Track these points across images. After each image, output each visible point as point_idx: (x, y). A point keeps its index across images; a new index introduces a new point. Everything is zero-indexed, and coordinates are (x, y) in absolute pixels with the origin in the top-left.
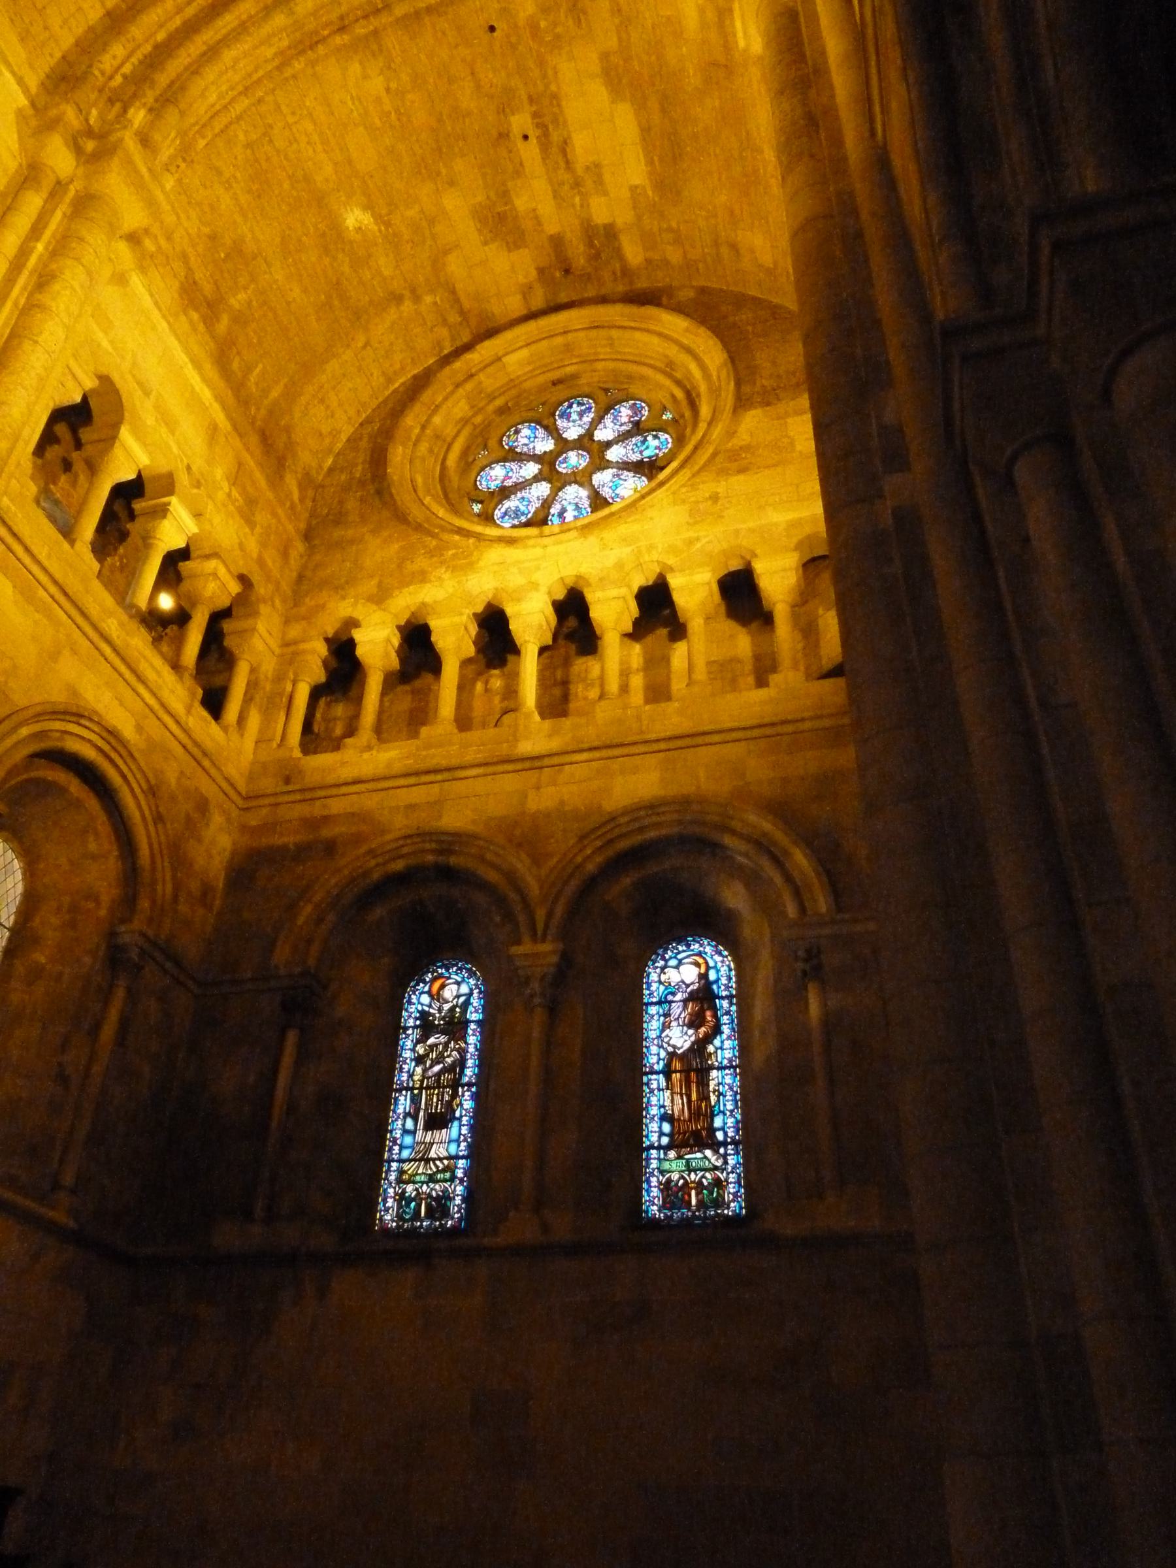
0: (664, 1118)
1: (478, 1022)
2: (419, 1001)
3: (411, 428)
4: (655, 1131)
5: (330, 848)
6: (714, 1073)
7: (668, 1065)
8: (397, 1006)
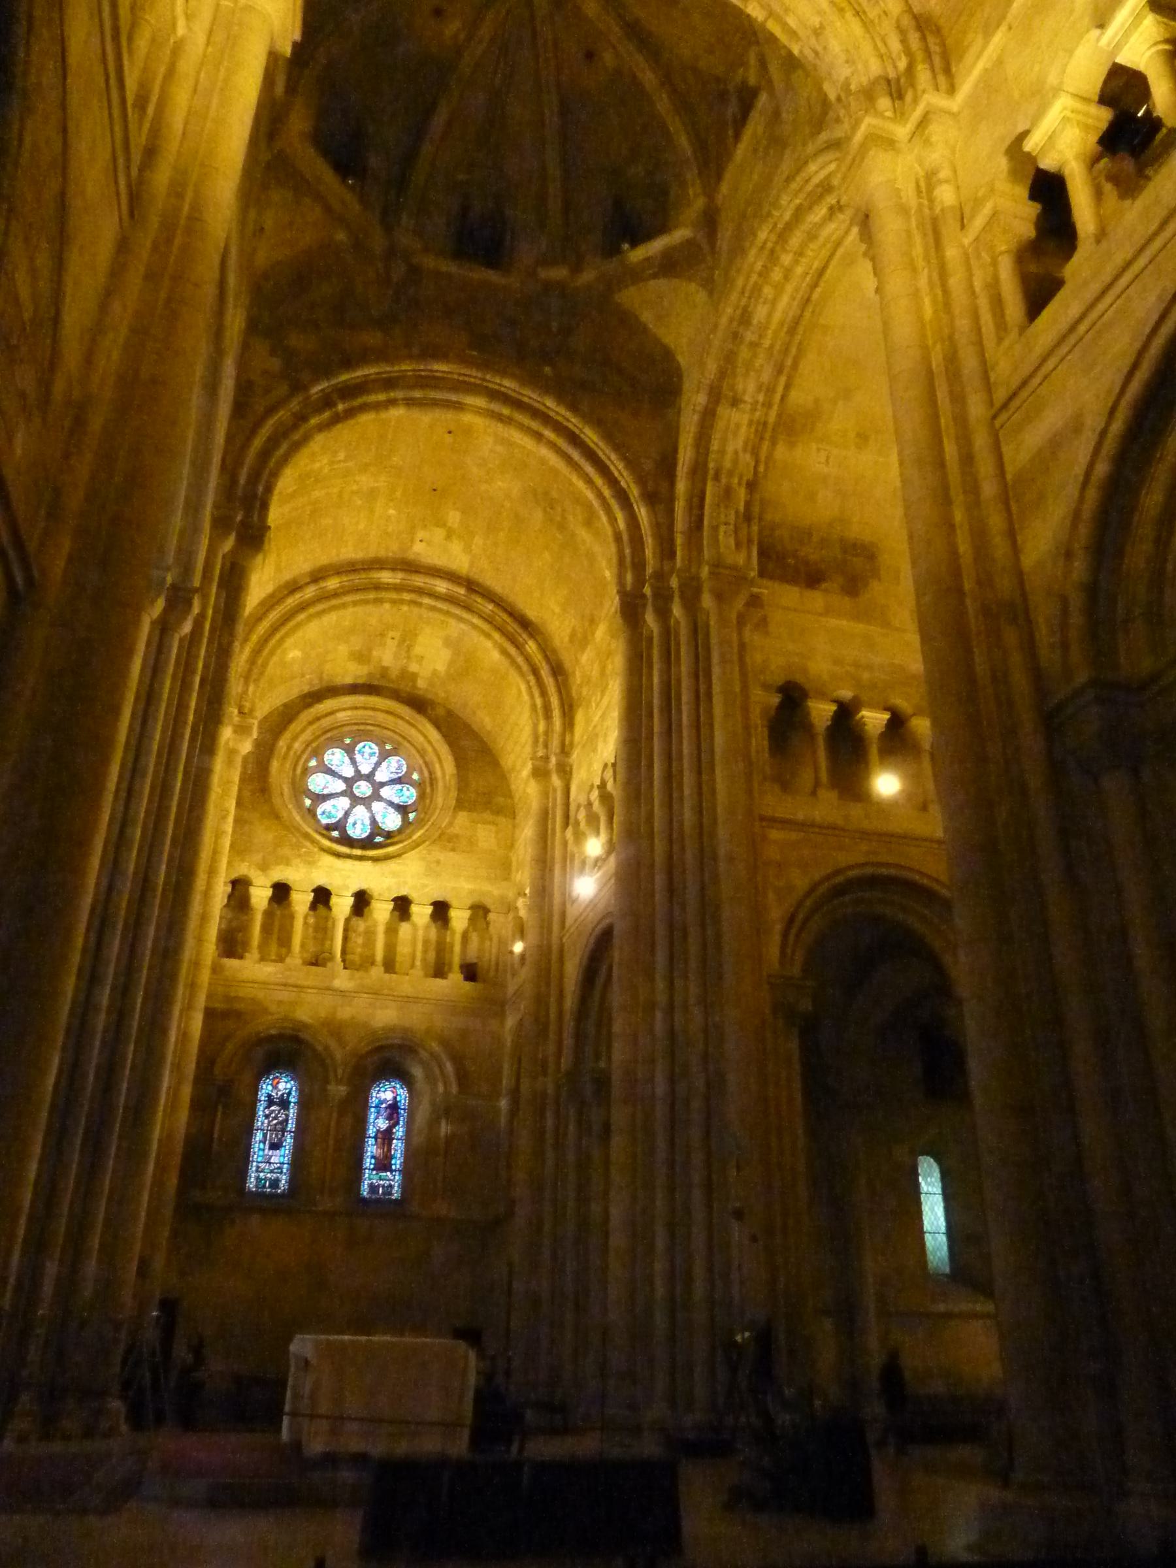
0: (373, 1157)
1: (294, 1103)
2: (266, 1088)
3: (282, 747)
4: (368, 1162)
5: (238, 1015)
6: (395, 1141)
7: (376, 1135)
8: (256, 1090)
